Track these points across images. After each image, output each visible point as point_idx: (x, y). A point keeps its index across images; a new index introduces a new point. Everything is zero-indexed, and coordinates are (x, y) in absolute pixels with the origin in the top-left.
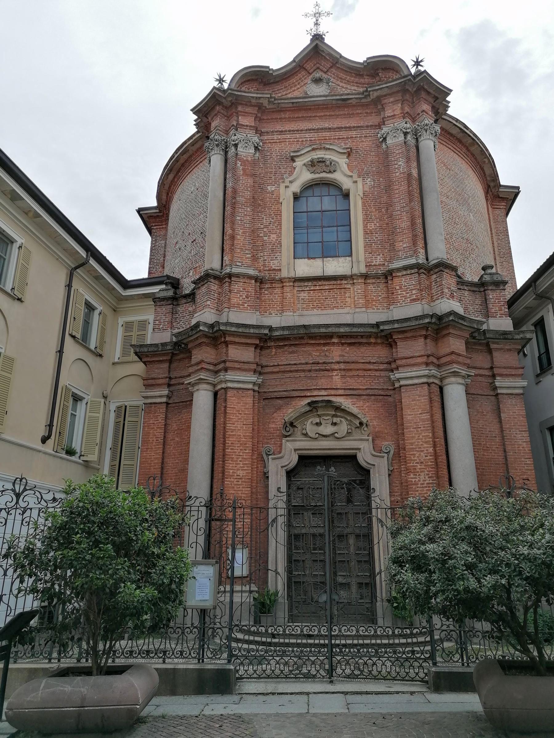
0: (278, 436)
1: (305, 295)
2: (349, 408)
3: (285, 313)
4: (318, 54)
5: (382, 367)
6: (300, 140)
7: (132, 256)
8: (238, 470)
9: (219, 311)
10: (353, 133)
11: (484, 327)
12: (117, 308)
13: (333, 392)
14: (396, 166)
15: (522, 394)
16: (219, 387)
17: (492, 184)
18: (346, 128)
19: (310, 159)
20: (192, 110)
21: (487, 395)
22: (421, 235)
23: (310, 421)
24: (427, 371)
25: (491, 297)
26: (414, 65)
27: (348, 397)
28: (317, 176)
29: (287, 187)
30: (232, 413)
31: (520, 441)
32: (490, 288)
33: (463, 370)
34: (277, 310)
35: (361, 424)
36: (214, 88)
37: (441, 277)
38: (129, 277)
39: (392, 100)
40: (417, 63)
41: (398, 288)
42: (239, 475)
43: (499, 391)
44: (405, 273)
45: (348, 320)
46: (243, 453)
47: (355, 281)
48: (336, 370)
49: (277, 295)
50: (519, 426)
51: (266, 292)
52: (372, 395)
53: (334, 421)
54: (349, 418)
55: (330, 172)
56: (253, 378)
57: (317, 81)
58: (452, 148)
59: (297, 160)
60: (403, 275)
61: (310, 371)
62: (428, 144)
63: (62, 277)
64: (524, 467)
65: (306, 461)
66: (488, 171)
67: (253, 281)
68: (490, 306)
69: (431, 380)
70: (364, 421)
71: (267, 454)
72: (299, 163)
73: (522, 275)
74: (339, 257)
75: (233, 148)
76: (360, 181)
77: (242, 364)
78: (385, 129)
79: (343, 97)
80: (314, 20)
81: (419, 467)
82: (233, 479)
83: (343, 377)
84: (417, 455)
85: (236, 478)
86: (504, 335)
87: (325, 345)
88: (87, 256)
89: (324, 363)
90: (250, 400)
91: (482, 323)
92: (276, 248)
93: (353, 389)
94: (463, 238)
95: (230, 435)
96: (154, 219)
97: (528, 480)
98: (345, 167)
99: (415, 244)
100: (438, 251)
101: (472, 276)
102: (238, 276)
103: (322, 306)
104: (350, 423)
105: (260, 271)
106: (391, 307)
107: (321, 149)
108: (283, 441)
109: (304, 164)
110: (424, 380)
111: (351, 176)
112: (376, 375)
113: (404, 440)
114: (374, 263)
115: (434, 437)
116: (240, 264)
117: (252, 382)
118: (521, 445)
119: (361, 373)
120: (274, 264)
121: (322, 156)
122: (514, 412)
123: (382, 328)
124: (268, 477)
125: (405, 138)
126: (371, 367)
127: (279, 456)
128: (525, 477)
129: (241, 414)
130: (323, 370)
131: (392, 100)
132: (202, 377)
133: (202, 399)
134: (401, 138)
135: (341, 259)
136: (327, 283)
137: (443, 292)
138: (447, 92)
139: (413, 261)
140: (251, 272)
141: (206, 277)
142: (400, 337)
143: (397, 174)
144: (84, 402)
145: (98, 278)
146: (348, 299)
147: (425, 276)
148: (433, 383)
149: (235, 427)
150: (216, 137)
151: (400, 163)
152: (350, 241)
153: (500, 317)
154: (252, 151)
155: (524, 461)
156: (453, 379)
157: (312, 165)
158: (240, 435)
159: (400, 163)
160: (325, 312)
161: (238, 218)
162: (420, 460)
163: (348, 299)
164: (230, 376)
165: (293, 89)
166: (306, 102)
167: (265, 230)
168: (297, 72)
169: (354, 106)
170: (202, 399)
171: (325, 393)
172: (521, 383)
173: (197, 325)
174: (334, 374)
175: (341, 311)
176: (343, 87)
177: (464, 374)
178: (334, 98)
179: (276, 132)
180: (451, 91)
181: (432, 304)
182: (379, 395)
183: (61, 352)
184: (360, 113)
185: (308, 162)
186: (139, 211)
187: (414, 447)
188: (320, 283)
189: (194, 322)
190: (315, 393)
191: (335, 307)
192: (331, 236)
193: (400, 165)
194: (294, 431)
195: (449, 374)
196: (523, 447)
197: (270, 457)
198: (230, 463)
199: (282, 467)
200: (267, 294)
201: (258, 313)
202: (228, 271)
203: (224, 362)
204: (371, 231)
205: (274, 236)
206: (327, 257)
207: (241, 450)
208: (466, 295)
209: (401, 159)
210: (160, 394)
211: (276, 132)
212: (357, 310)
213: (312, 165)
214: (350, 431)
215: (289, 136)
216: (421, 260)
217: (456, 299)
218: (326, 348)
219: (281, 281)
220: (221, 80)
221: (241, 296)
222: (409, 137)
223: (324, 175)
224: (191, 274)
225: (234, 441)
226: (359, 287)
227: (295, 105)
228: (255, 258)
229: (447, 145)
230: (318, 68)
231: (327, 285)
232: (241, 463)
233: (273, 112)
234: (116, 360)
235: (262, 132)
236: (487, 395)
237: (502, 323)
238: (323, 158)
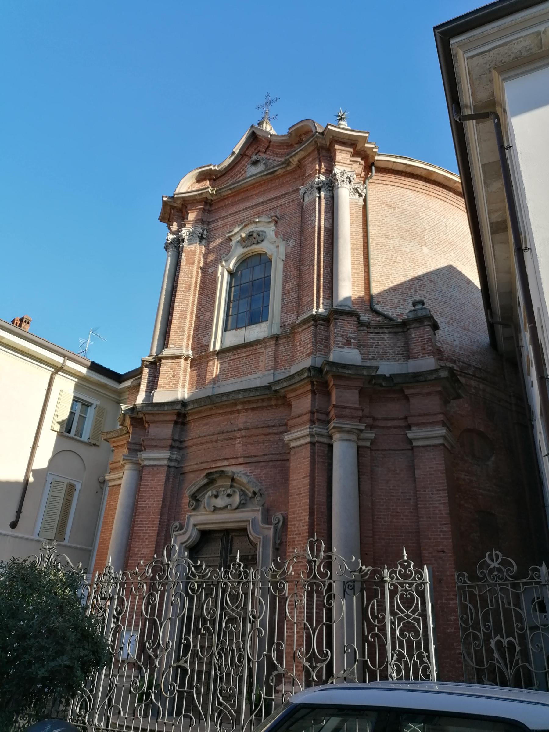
6: (239, 220)
8: (143, 548)
10: (282, 201)
12: (120, 400)
14: (310, 222)
18: (275, 198)
21: (403, 450)
25: (413, 336)
27: (247, 465)
28: (249, 249)
30: (145, 491)
32: (413, 326)
33: (347, 424)
38: (121, 371)
39: (310, 160)
41: (298, 344)
42: (143, 554)
43: (415, 444)
46: (150, 530)
48: (239, 438)
50: (436, 484)
52: (270, 461)
55: (258, 243)
57: (255, 163)
58: (400, 185)
61: (216, 441)
64: (440, 535)
68: (412, 346)
77: (158, 441)
79: (269, 171)
81: (297, 539)
83: (245, 444)
84: (297, 525)
87: (231, 412)
95: (140, 512)
97: (444, 552)
107: (251, 223)
112: (276, 439)
114: (288, 322)
117: (165, 459)
118: (437, 507)
119: (261, 438)
123: (273, 388)
126: (270, 431)
128: (440, 548)
129: (153, 491)
131: (310, 160)
142: (292, 395)
146: (261, 364)
147: (322, 327)
148: (317, 442)
149: (146, 504)
153: (422, 357)
155: (439, 528)
158: (150, 512)
160: (240, 380)
162: (298, 531)
166: (240, 185)
168: (240, 160)
169: (283, 176)
172: (438, 432)
174: (237, 442)
177: (349, 429)
178: (263, 174)
182: (277, 460)
184: (290, 181)
187: (295, 515)
188: (239, 351)
196: (440, 511)
198: (136, 542)
207: (149, 527)
208: (386, 338)
211: (220, 218)
217: (354, 346)
218: (232, 416)
225: (143, 518)
227: (233, 190)
229: (393, 184)
231: (244, 353)
232: (147, 540)
233: (219, 202)
235: (209, 222)
236: (403, 450)
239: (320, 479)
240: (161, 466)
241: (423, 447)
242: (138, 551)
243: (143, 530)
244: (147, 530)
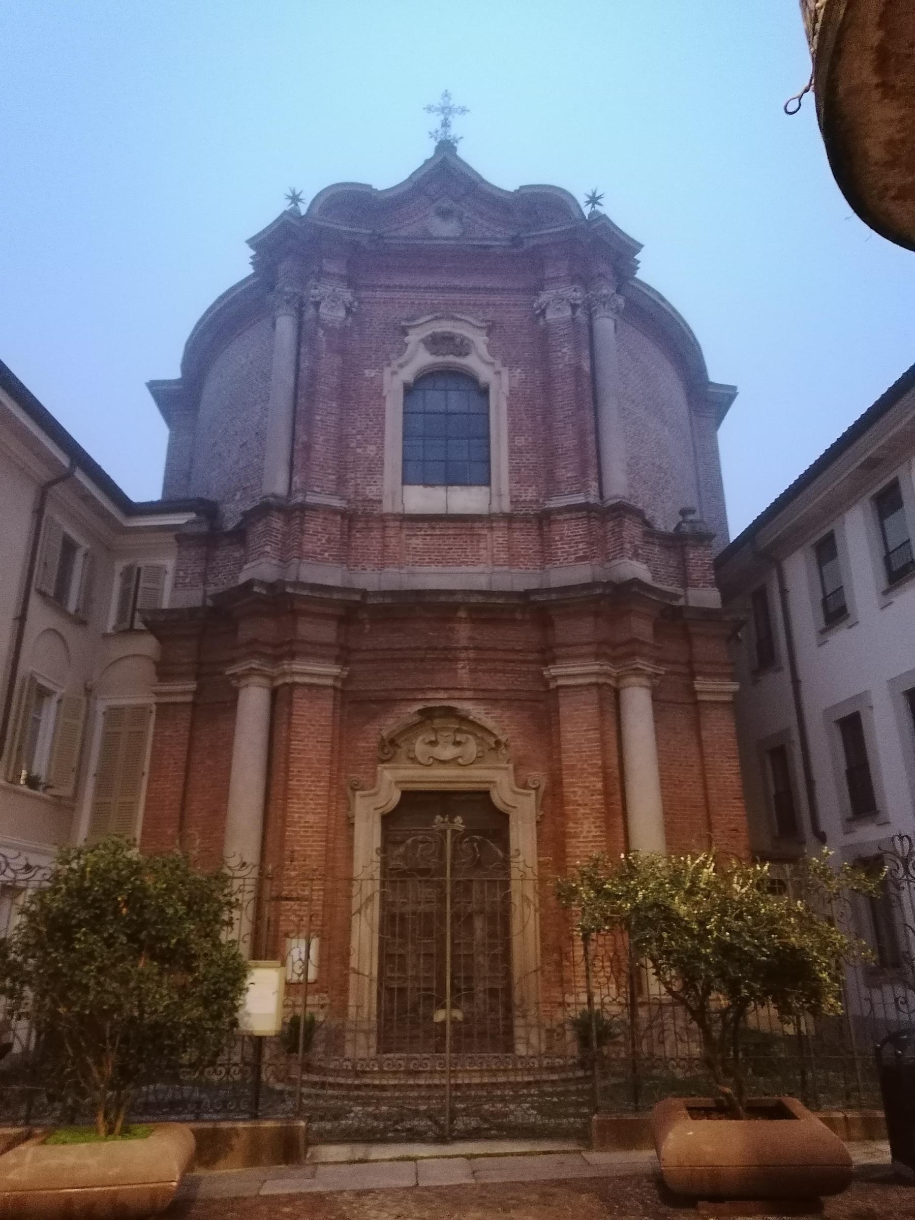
0: (370, 760)
1: (418, 542)
2: (480, 719)
3: (386, 570)
5: (531, 657)
6: (417, 302)
7: (136, 457)
8: (307, 813)
9: (284, 561)
10: (497, 299)
11: (681, 602)
13: (456, 694)
14: (560, 354)
15: (731, 702)
16: (280, 682)
19: (430, 332)
20: (247, 242)
22: (593, 462)
23: (420, 738)
24: (597, 667)
25: (691, 556)
26: (589, 202)
28: (440, 359)
29: (394, 373)
31: (727, 772)
32: (691, 542)
34: (375, 564)
35: (498, 743)
36: (285, 212)
37: (620, 525)
40: (594, 200)
43: (701, 697)
44: (568, 516)
45: (481, 583)
47: (494, 525)
48: (463, 660)
49: (374, 541)
51: (358, 535)
53: (458, 739)
54: (479, 735)
56: (335, 670)
57: (445, 214)
60: (565, 520)
61: (422, 660)
62: (605, 324)
63: (27, 499)
65: (416, 802)
67: (339, 518)
68: (690, 570)
69: (601, 680)
70: (503, 738)
71: (352, 789)
72: (413, 338)
73: (737, 523)
74: (471, 485)
76: (505, 372)
78: (544, 297)
80: (442, 117)
81: (582, 811)
82: (300, 827)
83: (472, 671)
85: (304, 827)
86: (707, 614)
88: (71, 465)
89: (445, 649)
90: (328, 704)
91: (676, 597)
92: (375, 467)
94: (653, 464)
98: (483, 349)
99: (584, 473)
100: (618, 484)
101: (665, 523)
102: (314, 508)
103: (444, 561)
104: (481, 742)
105: (349, 502)
106: (547, 566)
108: (379, 768)
110: (593, 680)
111: (492, 364)
116: (318, 490)
118: (728, 778)
119: (499, 666)
120: (371, 492)
121: (449, 330)
122: (720, 729)
124: (353, 824)
125: (574, 313)
127: (372, 791)
128: (733, 826)
130: (443, 660)
132: (254, 666)
133: (253, 701)
134: (568, 313)
135: (475, 490)
136: (451, 525)
137: (622, 549)
138: (636, 247)
139: (580, 499)
140: (336, 503)
141: (264, 509)
143: (561, 366)
144: (55, 698)
145: (87, 498)
146: (482, 552)
148: (605, 684)
149: (304, 746)
150: (287, 289)
151: (565, 350)
152: (488, 461)
153: (703, 587)
154: (342, 313)
156: (634, 680)
157: (436, 343)
159: (565, 350)
160: (447, 570)
161: (318, 418)
163: (482, 552)
164: (297, 666)
165: (407, 222)
167: (359, 437)
170: (253, 701)
171: (446, 696)
173: (249, 584)
174: (460, 666)
175: (470, 569)
179: (380, 287)
180: (641, 246)
181: (607, 565)
183: (22, 619)
185: (427, 337)
188: (441, 525)
189: (243, 578)
190: (430, 695)
191: (463, 562)
193: (565, 354)
194: (395, 753)
195: (631, 672)
197: (358, 793)
199: (376, 809)
200: (359, 538)
201: (345, 567)
202: (299, 498)
203: (290, 642)
204: (519, 448)
205: (373, 448)
206: (452, 485)
207: (313, 781)
209: (566, 344)
210: (183, 689)
211: (380, 287)
212: (497, 569)
213: (436, 343)
214: (480, 754)
215: (398, 295)
216: (592, 500)
219: (383, 519)
220: (295, 199)
221: (319, 540)
222: (579, 313)
223: (451, 358)
224: (237, 497)
226: (500, 534)
228: (341, 481)
234: (109, 630)
237: (707, 597)
238: (449, 333)
239: (611, 735)
240: (325, 687)
241: (711, 702)
242: (299, 817)
243: (303, 786)
244: (309, 786)
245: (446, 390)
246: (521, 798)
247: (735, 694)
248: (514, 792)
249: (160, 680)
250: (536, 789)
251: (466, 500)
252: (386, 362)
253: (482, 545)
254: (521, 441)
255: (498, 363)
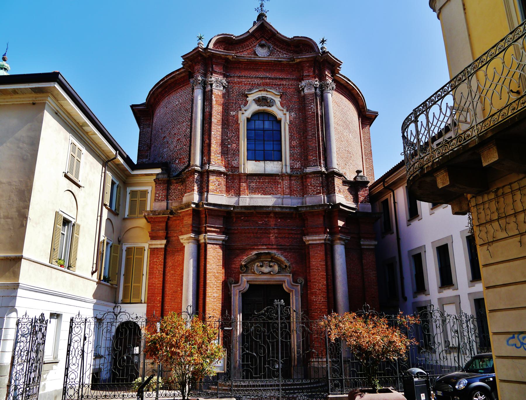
4: (263, 32)
8: (214, 293)
10: (284, 82)
17: (362, 110)
23: (256, 264)
28: (261, 108)
29: (243, 113)
40: (323, 41)
41: (309, 184)
44: (313, 175)
59: (249, 96)
66: (360, 103)
72: (250, 98)
74: (274, 161)
75: (209, 86)
76: (288, 113)
78: (303, 83)
88: (116, 153)
93: (282, 245)
94: (345, 150)
96: (143, 113)
98: (278, 103)
101: (351, 177)
107: (264, 91)
109: (254, 100)
113: (310, 276)
115: (327, 275)
125: (316, 90)
133: (189, 249)
135: (276, 163)
146: (279, 189)
151: (312, 106)
156: (338, 241)
157: (260, 101)
159: (312, 106)
163: (279, 189)
167: (229, 140)
176: (278, 51)
186: (132, 107)
192: (269, 147)
197: (233, 285)
199: (240, 291)
204: (294, 146)
205: (235, 145)
206: (267, 161)
210: (161, 243)
212: (285, 196)
213: (260, 101)
219: (240, 175)
223: (265, 108)
224: (177, 162)
226: (286, 182)
230: (263, 37)
234: (126, 216)
239: (329, 263)
245: (264, 121)
246: (295, 287)
247: (375, 245)
248: (293, 285)
249: (151, 239)
250: (301, 284)
251: (272, 167)
252: (239, 109)
253: (279, 186)
254: (294, 143)
255: (285, 110)
